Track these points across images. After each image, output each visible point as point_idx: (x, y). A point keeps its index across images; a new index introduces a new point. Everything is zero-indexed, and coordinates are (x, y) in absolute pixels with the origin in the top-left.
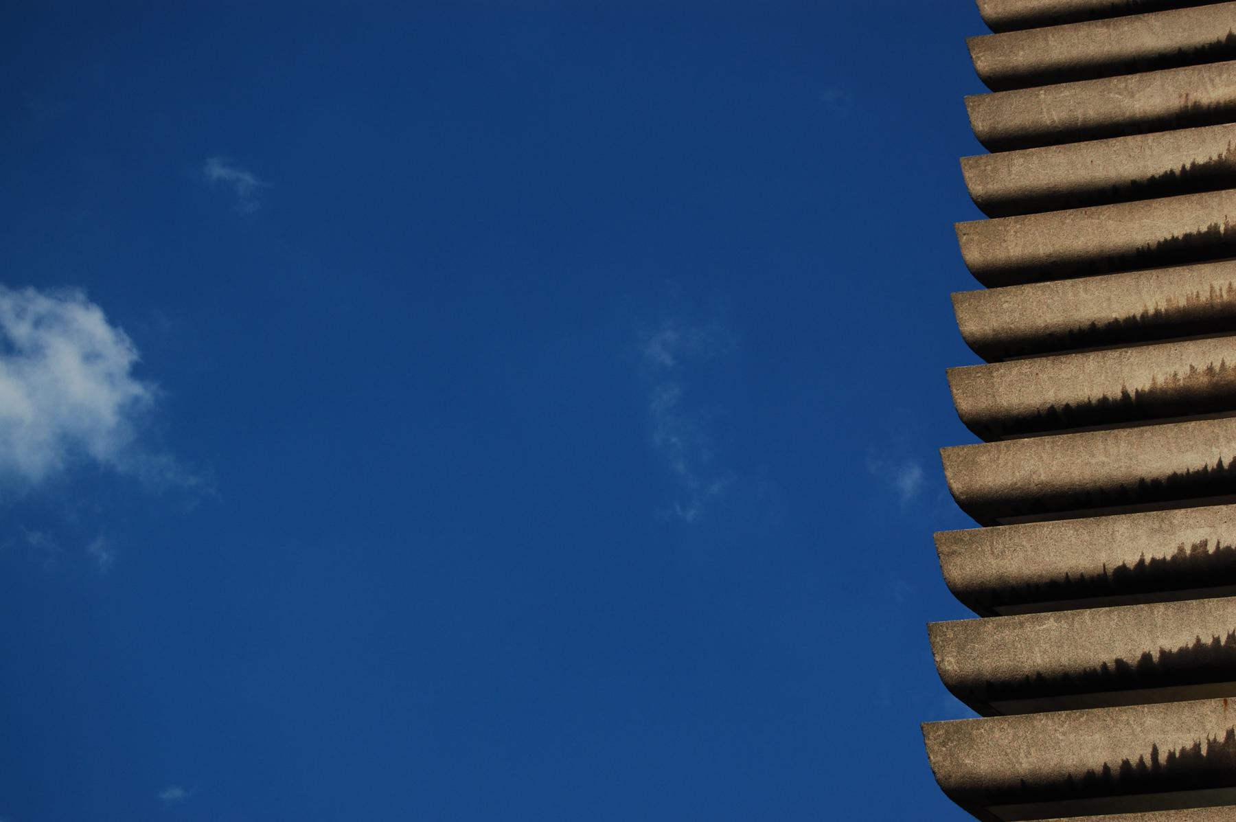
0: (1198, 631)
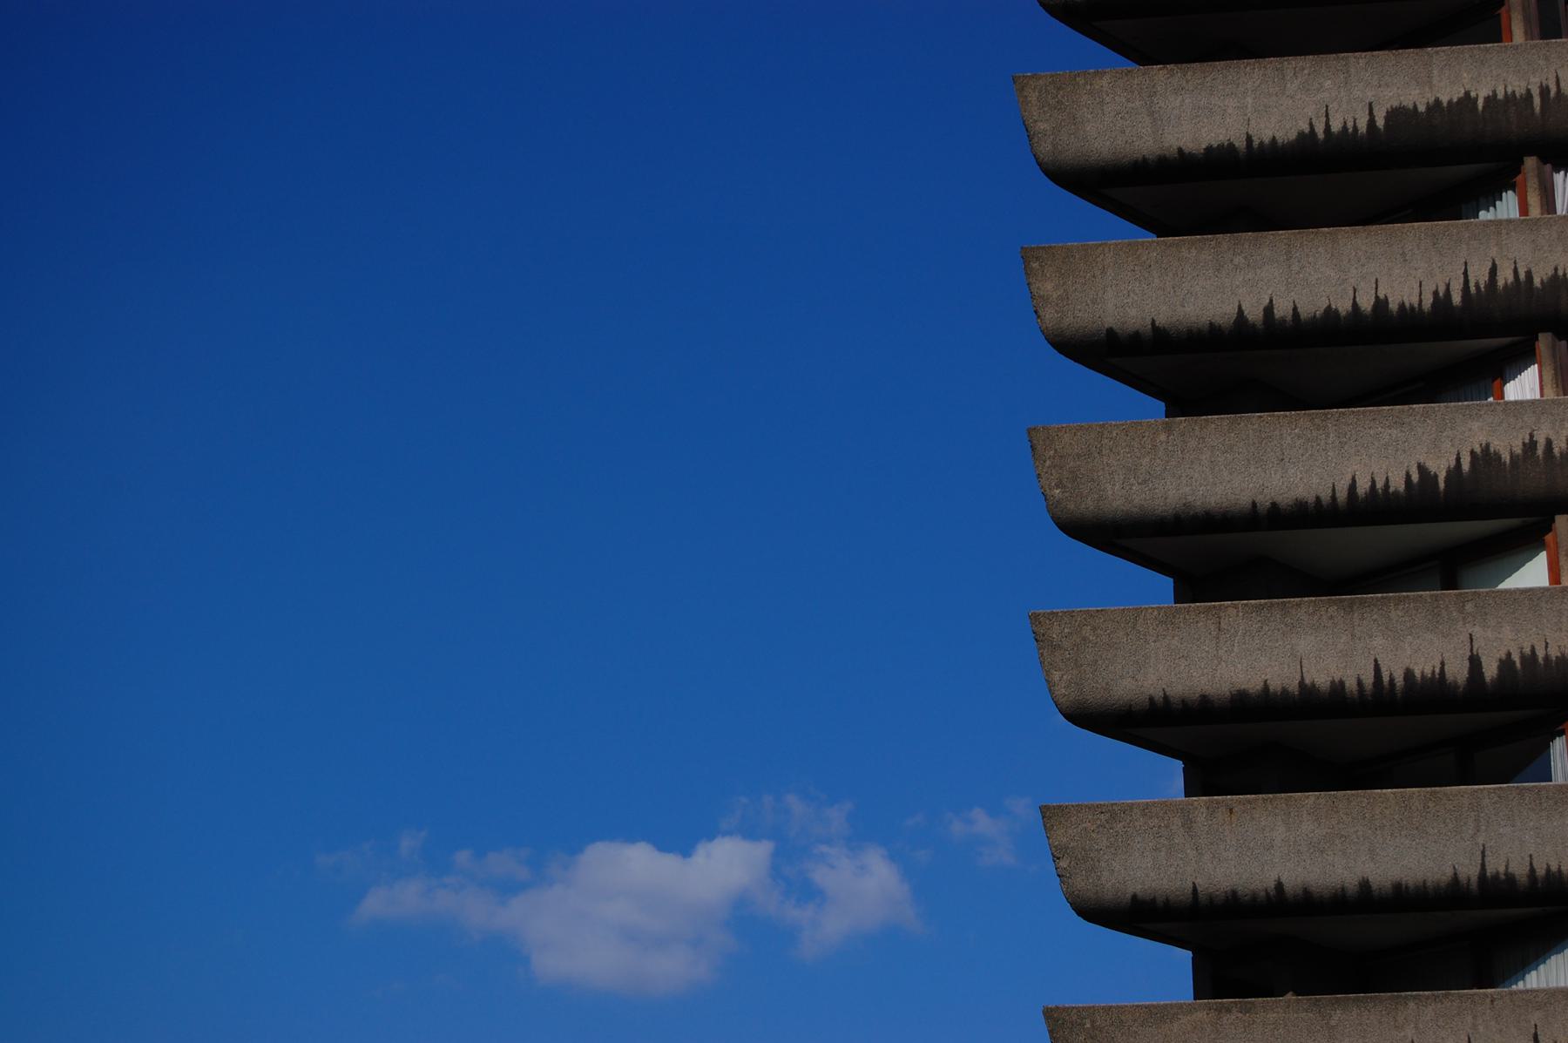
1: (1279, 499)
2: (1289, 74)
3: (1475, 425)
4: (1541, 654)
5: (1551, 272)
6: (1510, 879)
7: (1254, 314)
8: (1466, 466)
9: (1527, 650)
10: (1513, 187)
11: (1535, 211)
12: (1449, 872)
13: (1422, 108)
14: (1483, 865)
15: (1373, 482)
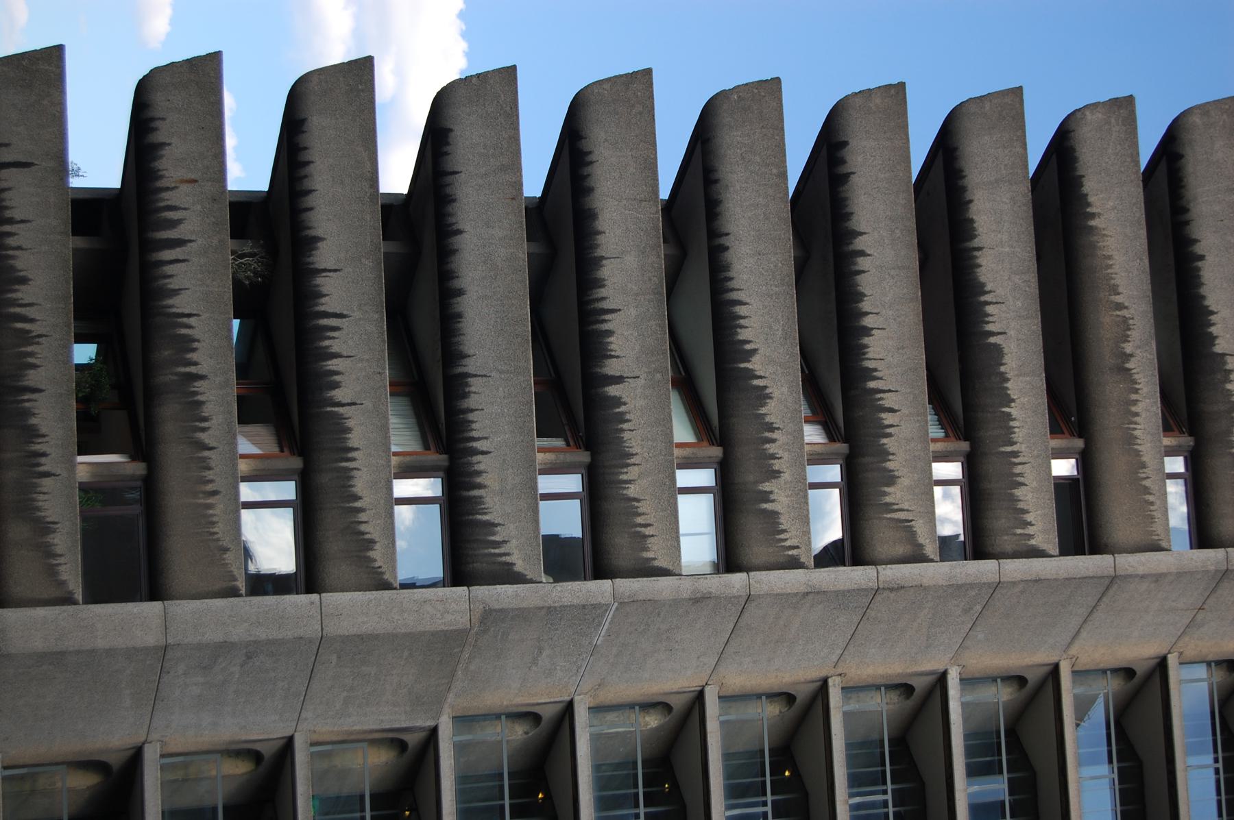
1: (731, 251)
2: (1026, 277)
3: (785, 389)
4: (625, 426)
5: (891, 450)
6: (465, 395)
7: (859, 243)
8: (756, 382)
9: (628, 417)
10: (947, 436)
11: (933, 447)
12: (471, 352)
13: (1002, 369)
14: (476, 376)
15: (744, 318)
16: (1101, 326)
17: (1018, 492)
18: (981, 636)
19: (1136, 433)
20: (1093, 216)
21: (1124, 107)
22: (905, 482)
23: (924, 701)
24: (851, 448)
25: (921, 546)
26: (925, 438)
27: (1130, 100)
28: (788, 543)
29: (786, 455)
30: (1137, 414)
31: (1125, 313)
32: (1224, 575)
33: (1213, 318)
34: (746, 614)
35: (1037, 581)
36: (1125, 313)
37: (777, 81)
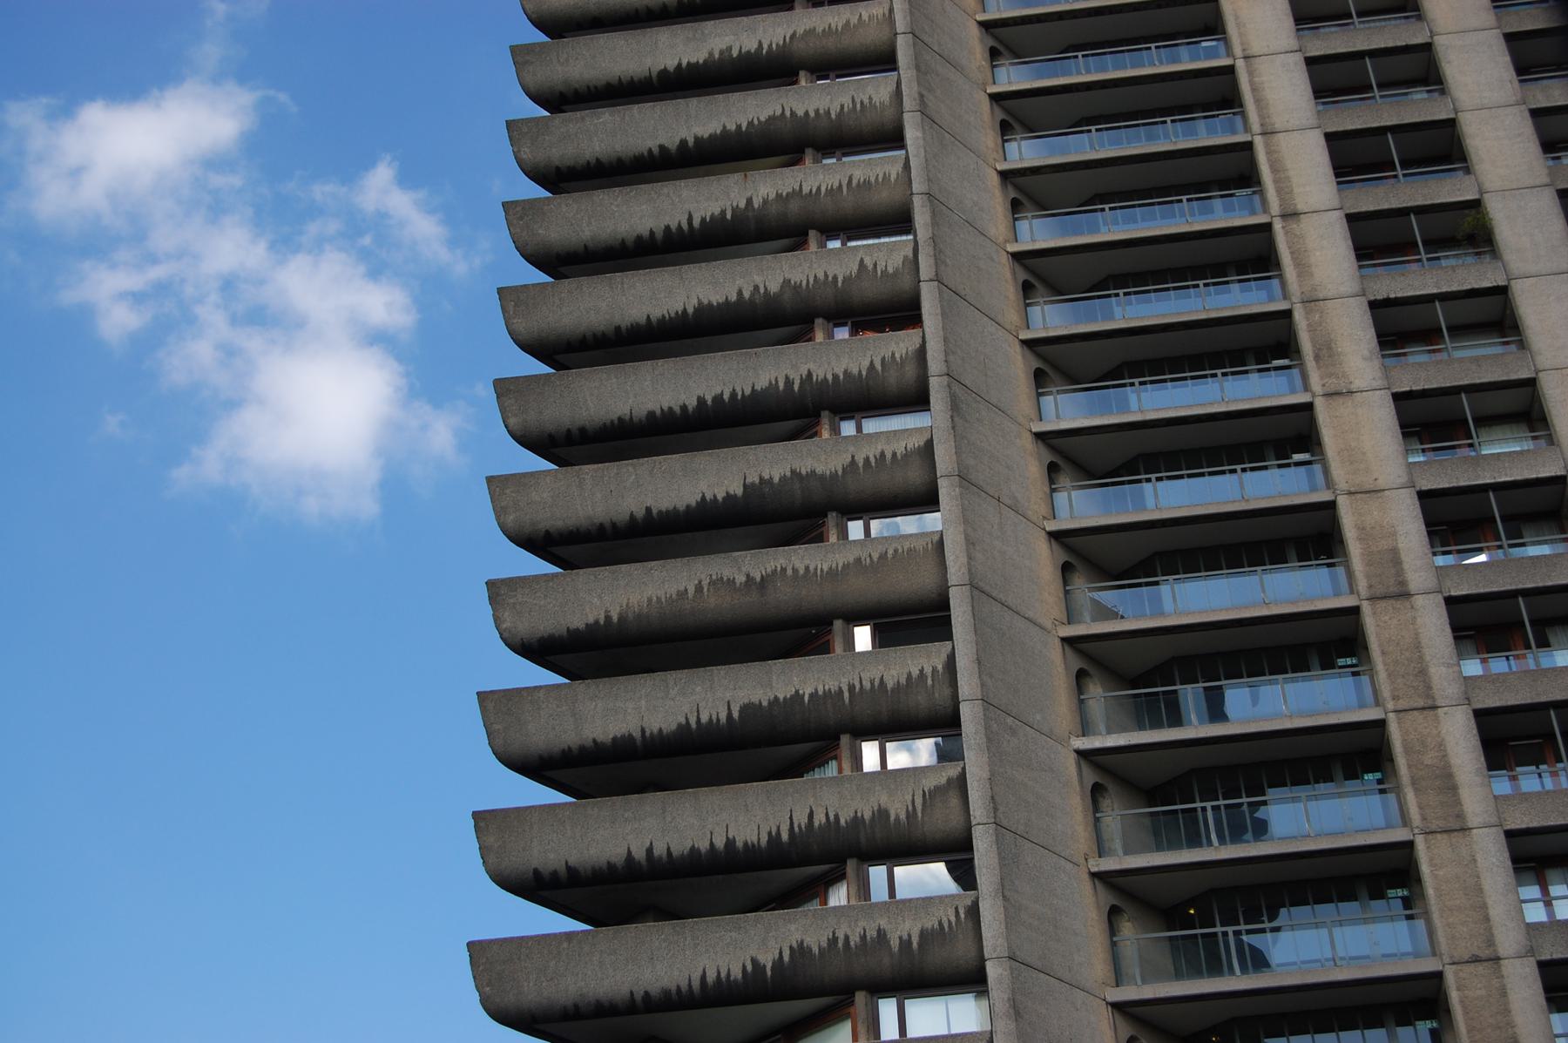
0: (724, 119)
1: (649, 989)
2: (671, 683)
3: (793, 927)
7: (639, 854)
8: (786, 958)
10: (835, 758)
11: (847, 771)
13: (765, 703)
16: (718, 605)
17: (890, 684)
18: (1038, 717)
19: (825, 568)
20: (608, 618)
21: (498, 591)
22: (884, 800)
23: (1108, 773)
24: (851, 856)
25: (949, 781)
26: (838, 780)
27: (491, 584)
28: (953, 919)
29: (862, 924)
30: (807, 568)
31: (705, 583)
32: (963, 478)
33: (709, 497)
34: (1029, 960)
35: (979, 662)
36: (705, 583)
37: (470, 945)
